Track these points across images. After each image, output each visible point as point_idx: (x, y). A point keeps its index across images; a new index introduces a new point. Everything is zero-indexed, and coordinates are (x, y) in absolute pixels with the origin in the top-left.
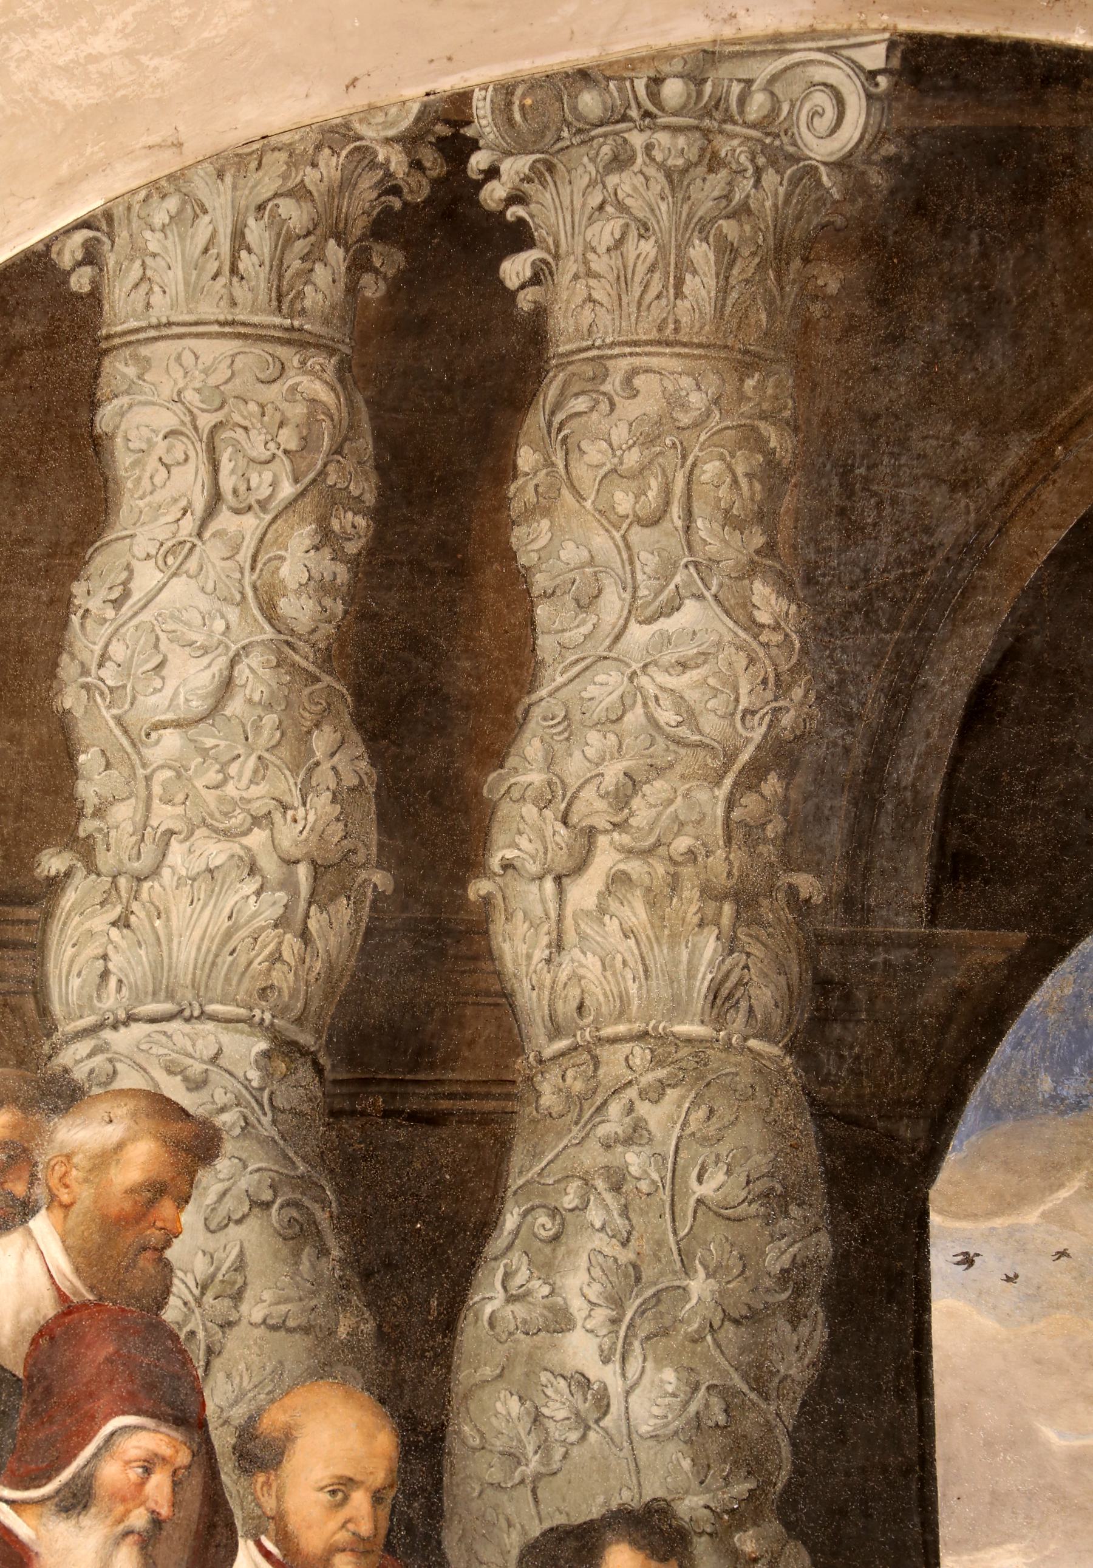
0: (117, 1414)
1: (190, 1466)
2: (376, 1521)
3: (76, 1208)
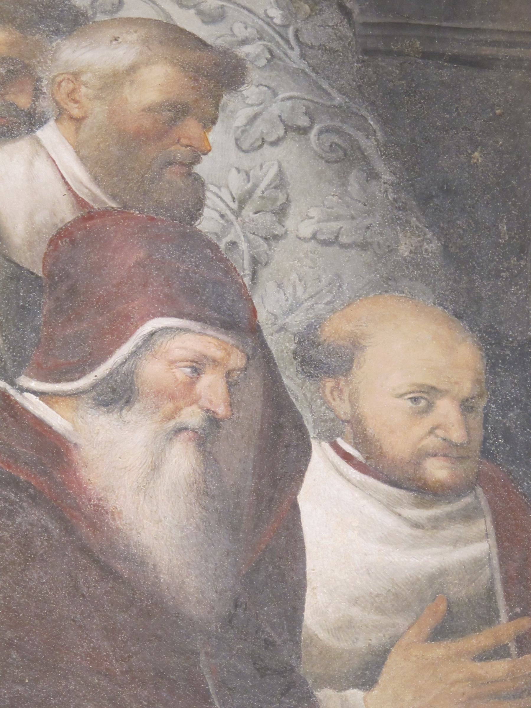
0: (155, 316)
1: (246, 369)
2: (468, 430)
3: (88, 121)
